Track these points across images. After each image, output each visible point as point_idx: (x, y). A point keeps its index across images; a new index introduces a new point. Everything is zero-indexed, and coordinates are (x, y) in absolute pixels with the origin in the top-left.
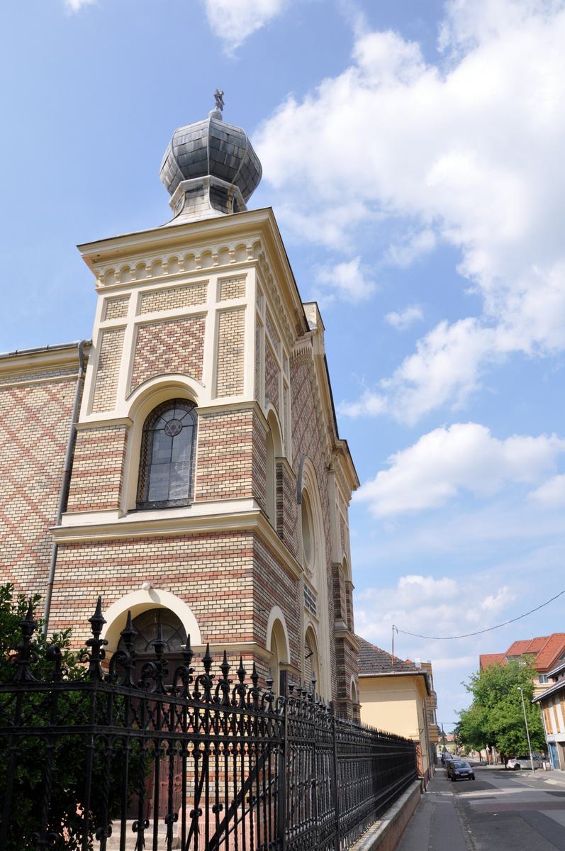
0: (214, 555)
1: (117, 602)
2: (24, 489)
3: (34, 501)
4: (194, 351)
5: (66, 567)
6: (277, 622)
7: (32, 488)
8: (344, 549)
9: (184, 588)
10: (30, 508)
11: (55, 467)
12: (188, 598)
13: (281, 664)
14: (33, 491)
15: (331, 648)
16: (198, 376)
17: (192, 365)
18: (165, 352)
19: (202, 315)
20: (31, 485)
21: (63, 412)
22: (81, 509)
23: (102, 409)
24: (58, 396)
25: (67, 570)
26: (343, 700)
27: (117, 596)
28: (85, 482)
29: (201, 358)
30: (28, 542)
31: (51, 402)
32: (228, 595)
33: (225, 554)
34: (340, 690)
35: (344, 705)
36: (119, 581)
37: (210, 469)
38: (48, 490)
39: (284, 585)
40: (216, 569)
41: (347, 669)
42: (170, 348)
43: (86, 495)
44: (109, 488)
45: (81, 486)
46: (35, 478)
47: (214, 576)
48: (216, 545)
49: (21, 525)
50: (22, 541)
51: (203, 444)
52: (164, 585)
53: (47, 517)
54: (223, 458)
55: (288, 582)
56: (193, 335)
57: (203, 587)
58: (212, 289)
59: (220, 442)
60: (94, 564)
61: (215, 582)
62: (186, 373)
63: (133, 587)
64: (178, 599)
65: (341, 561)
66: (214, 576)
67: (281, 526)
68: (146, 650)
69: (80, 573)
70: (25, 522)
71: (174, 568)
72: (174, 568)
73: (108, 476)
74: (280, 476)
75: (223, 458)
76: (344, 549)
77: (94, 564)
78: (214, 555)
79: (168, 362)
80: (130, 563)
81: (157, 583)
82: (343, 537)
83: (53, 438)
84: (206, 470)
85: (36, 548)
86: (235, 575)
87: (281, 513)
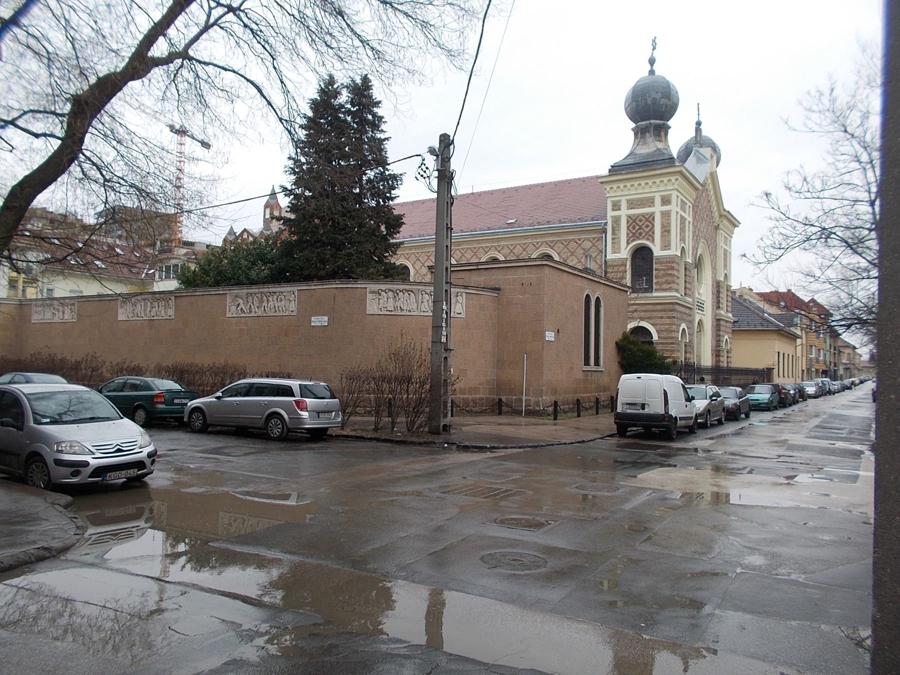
0: (662, 311)
4: (651, 229)
6: (684, 329)
8: (725, 266)
12: (653, 325)
15: (712, 325)
16: (653, 241)
17: (650, 236)
18: (639, 229)
19: (652, 215)
26: (718, 348)
29: (653, 233)
32: (666, 324)
35: (719, 351)
39: (686, 314)
41: (721, 333)
47: (662, 318)
51: (656, 270)
54: (664, 276)
55: (688, 311)
56: (650, 222)
57: (658, 321)
58: (658, 201)
59: (663, 270)
62: (648, 239)
65: (722, 279)
66: (662, 318)
71: (648, 314)
72: (648, 314)
74: (686, 269)
75: (664, 276)
76: (725, 266)
78: (662, 311)
79: (640, 234)
81: (642, 319)
82: (725, 260)
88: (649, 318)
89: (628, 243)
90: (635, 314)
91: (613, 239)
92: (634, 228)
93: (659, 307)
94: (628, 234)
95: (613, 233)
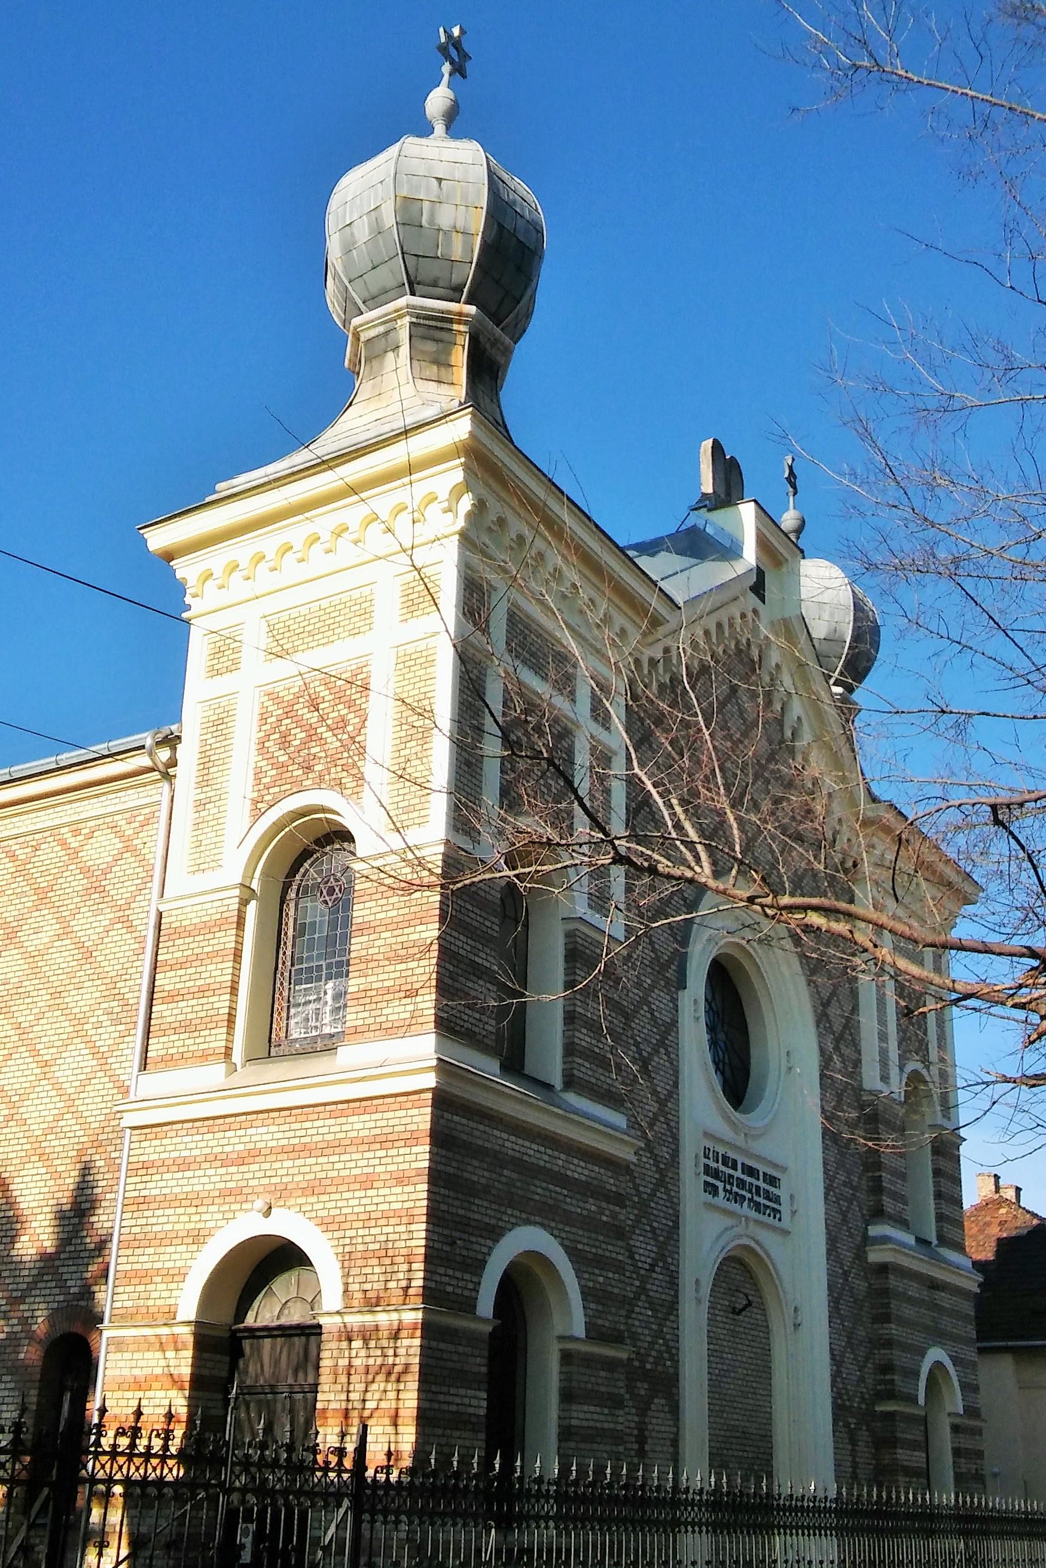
1: (218, 1233)
2: (86, 1027)
3: (102, 1049)
5: (144, 1172)
7: (99, 1025)
9: (326, 1205)
10: (95, 1062)
11: (132, 983)
12: (326, 1224)
13: (561, 1338)
14: (100, 1031)
20: (95, 1019)
21: (145, 874)
22: (169, 1061)
23: (202, 867)
24: (135, 842)
25: (145, 1179)
27: (220, 1224)
28: (175, 1012)
30: (93, 1126)
31: (125, 856)
33: (384, 1141)
34: (880, 1383)
36: (226, 1194)
37: (369, 979)
38: (122, 1027)
40: (371, 1170)
42: (312, 735)
43: (176, 1037)
44: (208, 1022)
45: (169, 1020)
46: (103, 1006)
47: (367, 1182)
48: (372, 1124)
49: (82, 1095)
50: (84, 1124)
52: (292, 1202)
53: (122, 1078)
57: (354, 1202)
60: (184, 1165)
61: (370, 1193)
63: (244, 1206)
64: (311, 1224)
66: (367, 1182)
67: (570, 1059)
68: (278, 1318)
69: (163, 1184)
70: (88, 1088)
73: (211, 1000)
77: (184, 1165)
80: (241, 1160)
83: (130, 928)
84: (363, 980)
85: (105, 1136)
86: (401, 1180)
87: (570, 1033)
88: (312, 1189)
89: (257, 814)
90: (253, 1174)
91: (200, 805)
92: (285, 741)
93: (360, 1124)
94: (258, 775)
95: (204, 782)
